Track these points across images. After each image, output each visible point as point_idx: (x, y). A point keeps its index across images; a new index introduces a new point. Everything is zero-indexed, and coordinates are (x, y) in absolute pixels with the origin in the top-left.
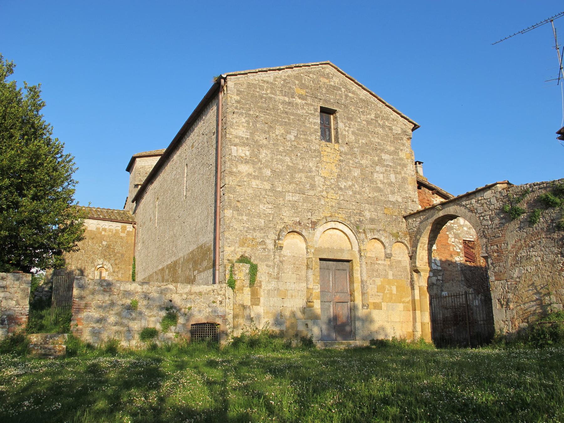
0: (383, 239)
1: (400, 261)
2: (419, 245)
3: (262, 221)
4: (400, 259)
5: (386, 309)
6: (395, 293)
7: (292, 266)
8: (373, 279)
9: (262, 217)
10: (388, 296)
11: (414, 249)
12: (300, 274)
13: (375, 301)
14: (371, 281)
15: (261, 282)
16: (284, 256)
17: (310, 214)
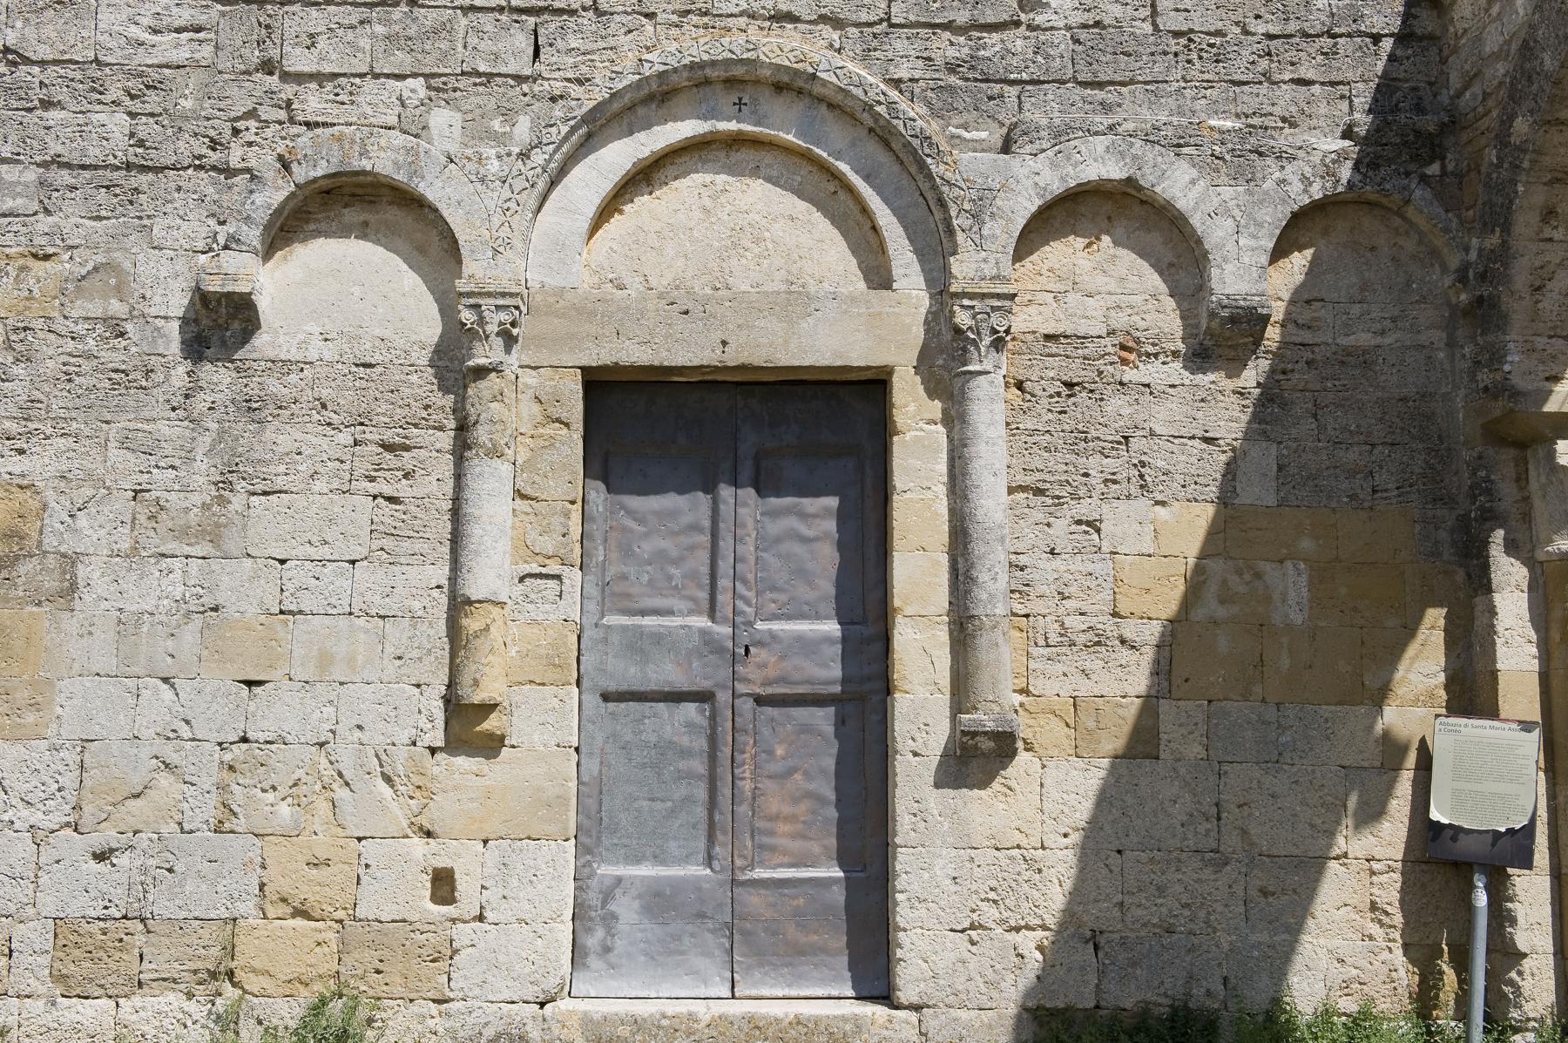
0: (1180, 184)
1: (1364, 360)
2: (1530, 197)
3: (117, 124)
4: (1363, 339)
5: (1195, 750)
6: (1297, 618)
7: (345, 437)
8: (1085, 509)
9: (114, 93)
10: (1223, 644)
11: (1494, 240)
12: (402, 489)
13: (1085, 688)
14: (1061, 526)
15: (70, 561)
16: (284, 366)
17: (523, 42)
